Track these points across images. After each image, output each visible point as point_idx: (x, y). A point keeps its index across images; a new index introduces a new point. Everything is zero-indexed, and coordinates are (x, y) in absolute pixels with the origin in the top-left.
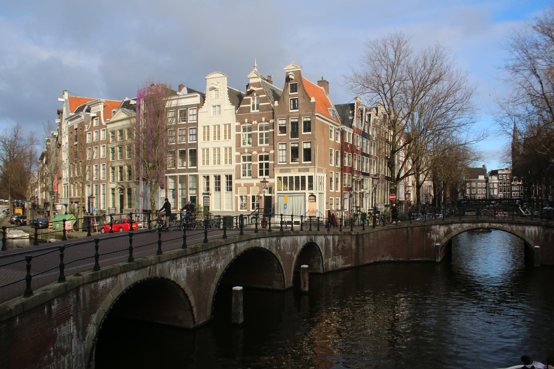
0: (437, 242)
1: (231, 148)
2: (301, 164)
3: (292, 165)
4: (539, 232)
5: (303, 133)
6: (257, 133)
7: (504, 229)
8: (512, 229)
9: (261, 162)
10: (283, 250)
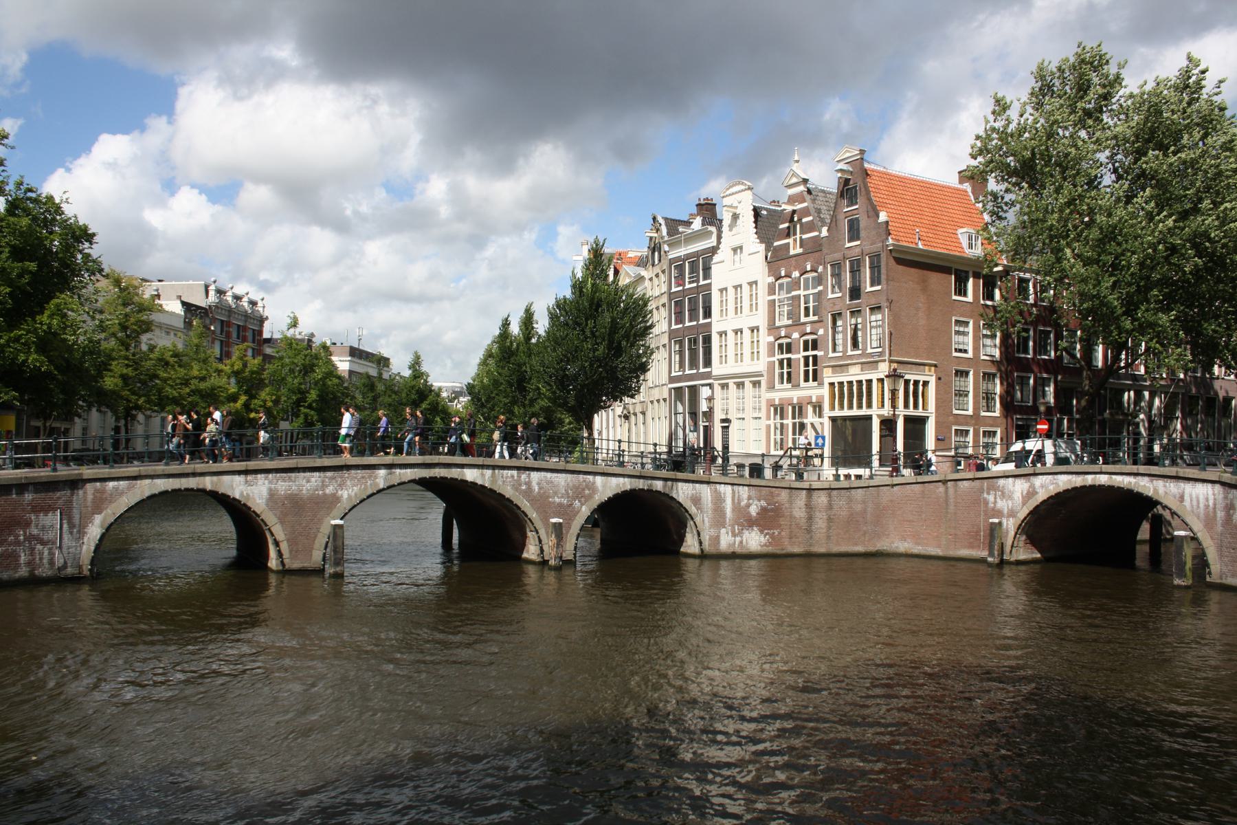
1: (758, 330)
2: (864, 354)
5: (869, 289)
8: (1156, 490)
9: (807, 354)
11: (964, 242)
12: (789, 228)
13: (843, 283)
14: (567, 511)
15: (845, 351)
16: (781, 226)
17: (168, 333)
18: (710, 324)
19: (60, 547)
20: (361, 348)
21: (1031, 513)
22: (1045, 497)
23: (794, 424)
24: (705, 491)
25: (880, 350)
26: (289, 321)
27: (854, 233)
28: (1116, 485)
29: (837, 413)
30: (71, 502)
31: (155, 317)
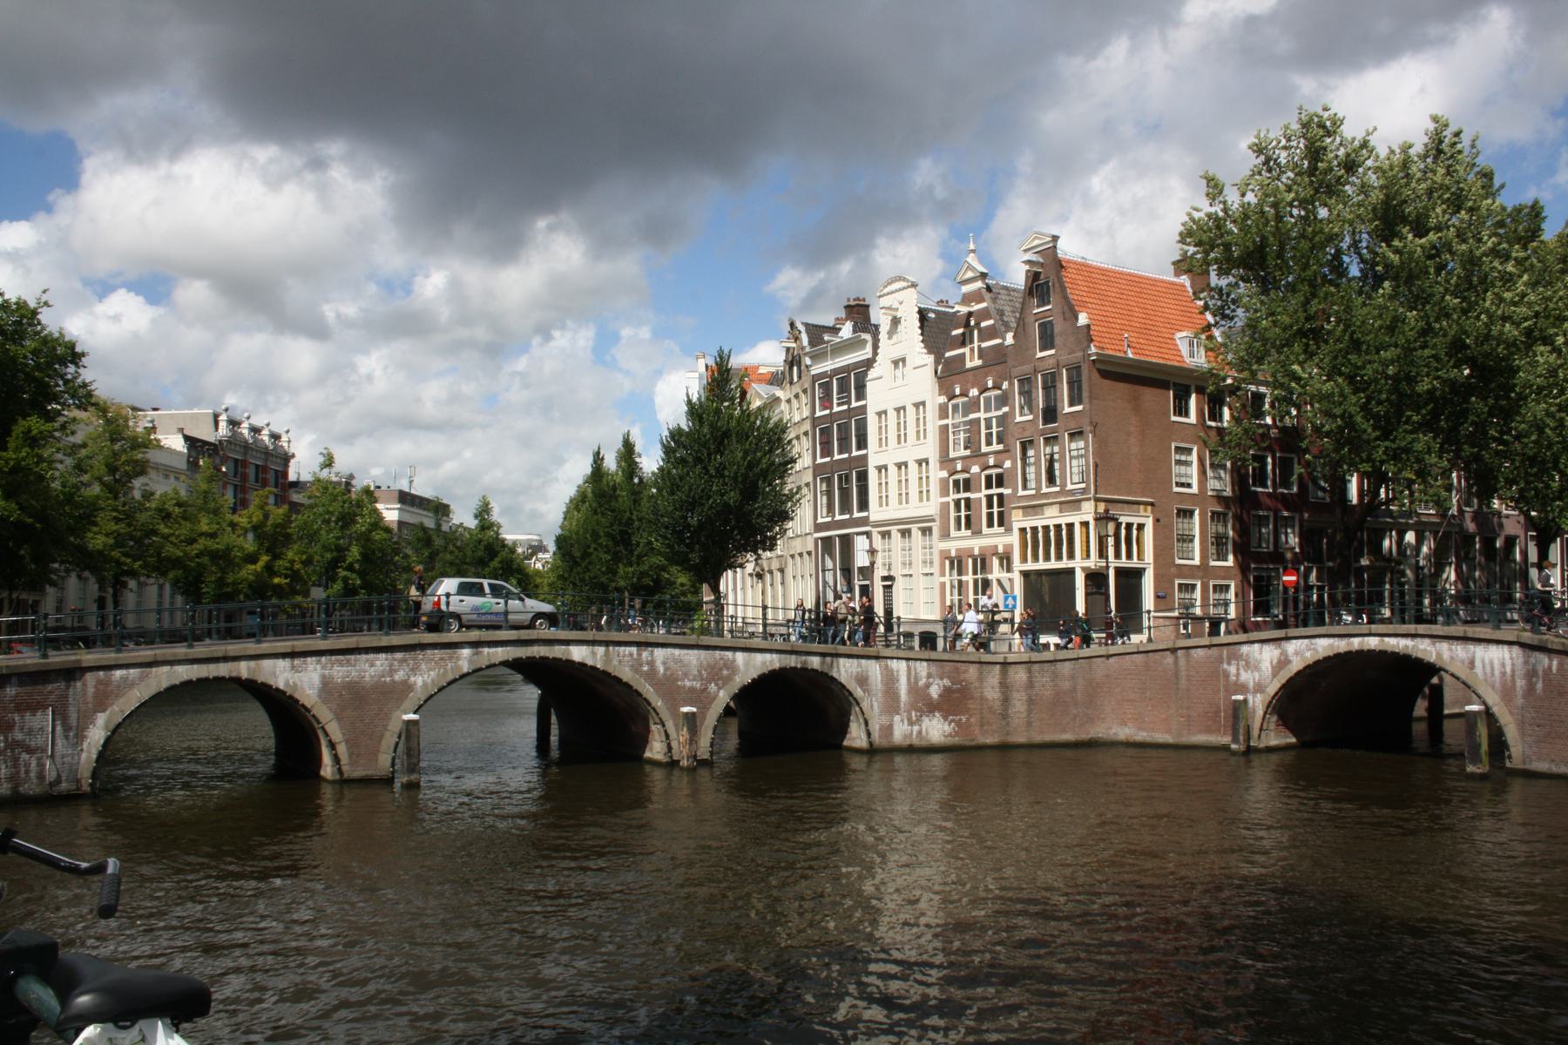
1: (927, 463)
2: (1063, 492)
3: (1046, 495)
4: (1513, 665)
5: (1067, 410)
6: (978, 420)
8: (1439, 655)
10: (665, 674)
11: (1184, 348)
12: (963, 334)
13: (1034, 403)
14: (701, 698)
15: (1038, 488)
16: (955, 332)
17: (167, 477)
18: (865, 457)
19: (52, 756)
20: (413, 492)
21: (1283, 687)
23: (976, 582)
24: (874, 669)
25: (1083, 485)
26: (321, 459)
27: (1047, 341)
28: (1389, 649)
29: (1030, 566)
30: (66, 697)
31: (153, 456)
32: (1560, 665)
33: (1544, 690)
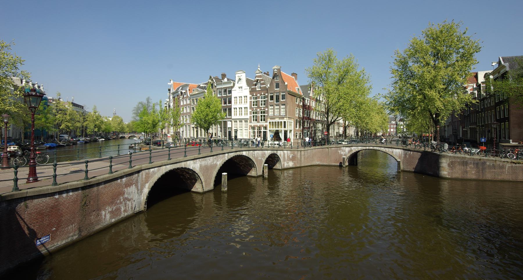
0: (344, 156)
1: (247, 108)
5: (281, 100)
6: (259, 100)
7: (382, 150)
8: (386, 150)
12: (256, 84)
14: (261, 160)
16: (254, 83)
18: (231, 106)
22: (355, 152)
23: (258, 132)
27: (277, 86)
32: (413, 153)
33: (409, 157)
